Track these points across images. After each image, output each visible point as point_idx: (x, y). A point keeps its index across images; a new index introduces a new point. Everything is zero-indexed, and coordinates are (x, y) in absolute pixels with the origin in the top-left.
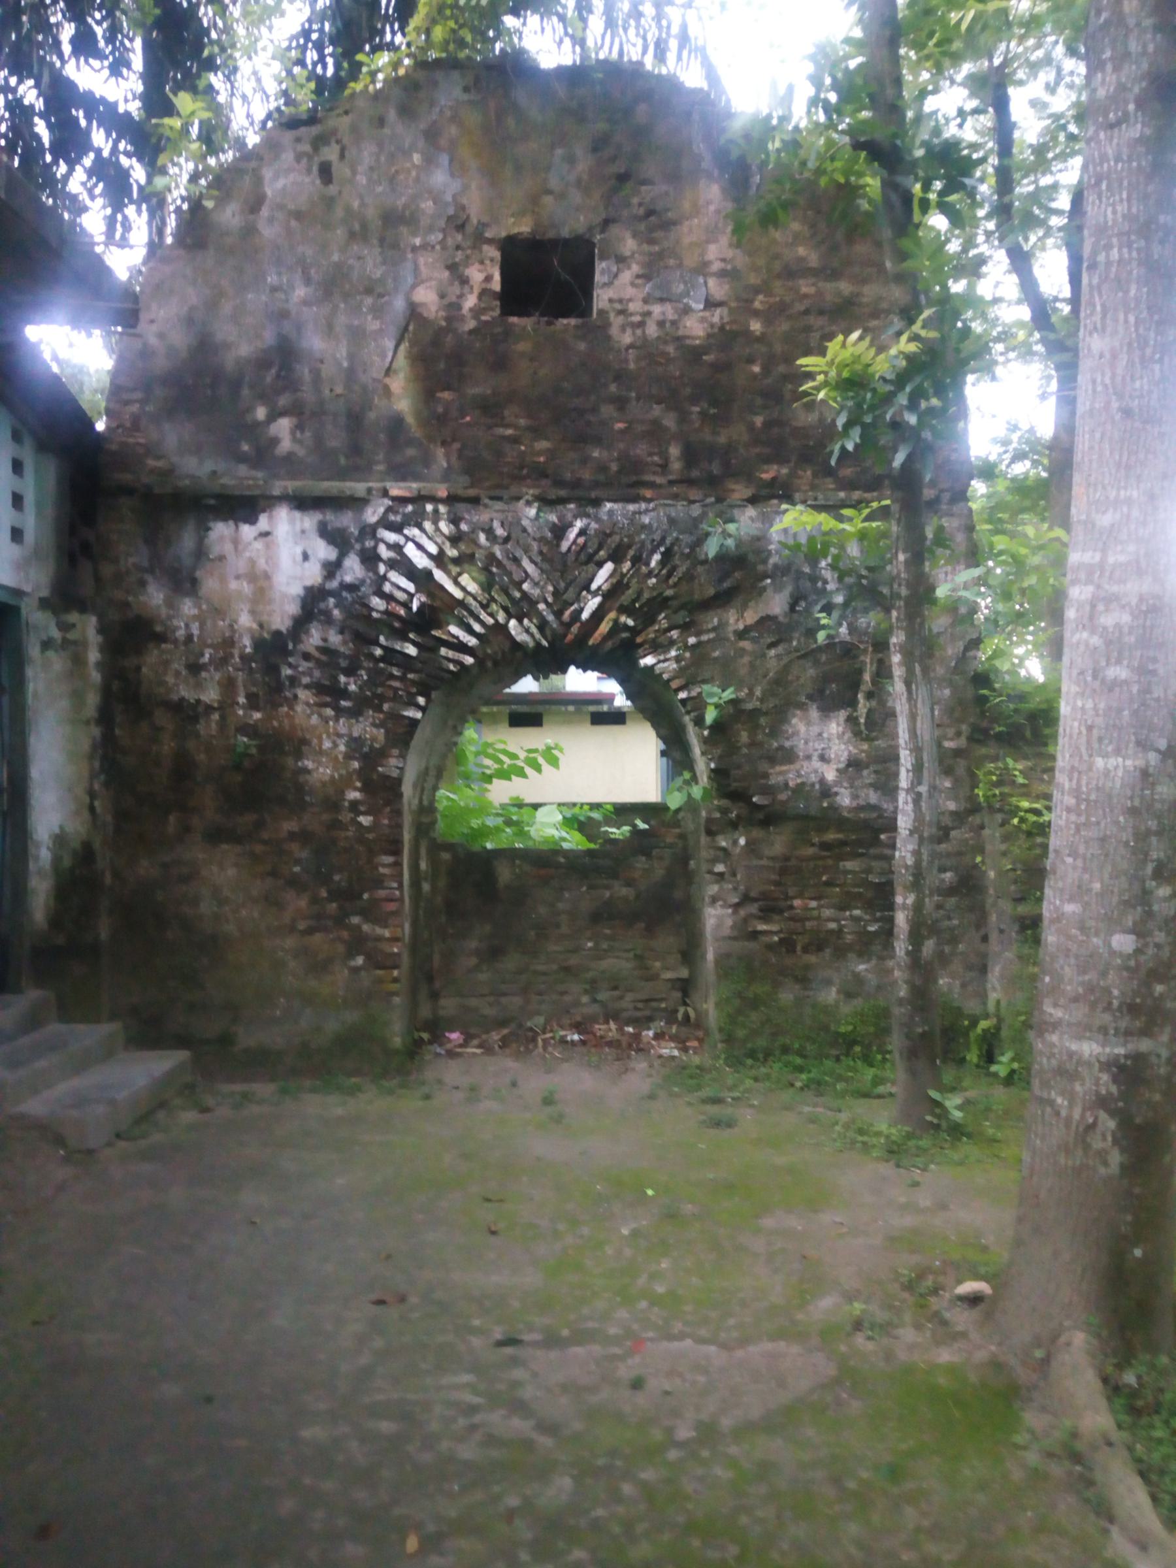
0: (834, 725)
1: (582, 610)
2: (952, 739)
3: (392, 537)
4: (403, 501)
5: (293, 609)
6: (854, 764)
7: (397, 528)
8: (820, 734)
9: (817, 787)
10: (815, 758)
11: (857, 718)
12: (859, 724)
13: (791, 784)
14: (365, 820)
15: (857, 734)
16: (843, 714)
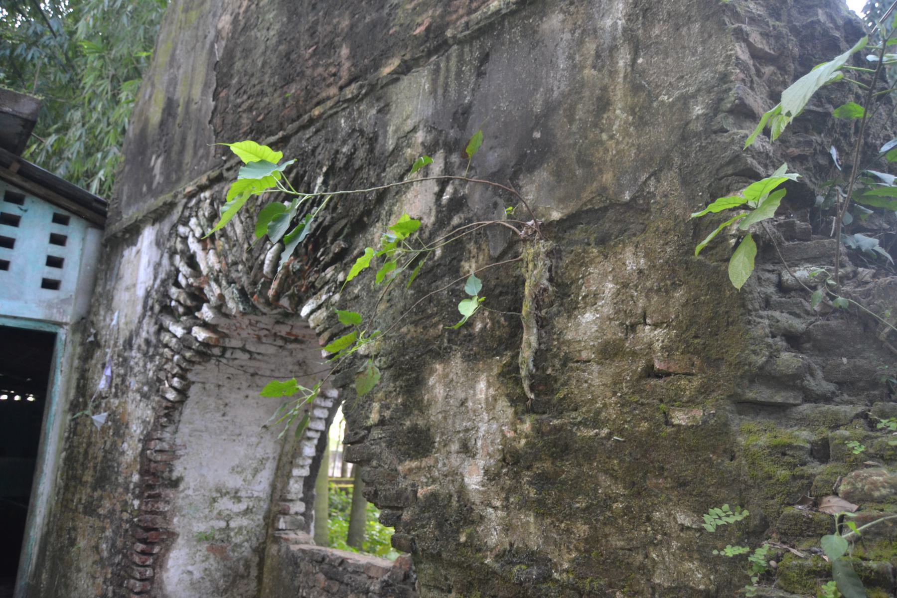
0: (482, 385)
1: (263, 262)
2: (692, 402)
3: (182, 230)
4: (191, 196)
5: (139, 309)
6: (512, 460)
7: (186, 223)
8: (463, 403)
9: (454, 503)
10: (455, 447)
11: (517, 369)
12: (518, 382)
13: (421, 492)
14: (136, 503)
15: (516, 400)
16: (498, 363)
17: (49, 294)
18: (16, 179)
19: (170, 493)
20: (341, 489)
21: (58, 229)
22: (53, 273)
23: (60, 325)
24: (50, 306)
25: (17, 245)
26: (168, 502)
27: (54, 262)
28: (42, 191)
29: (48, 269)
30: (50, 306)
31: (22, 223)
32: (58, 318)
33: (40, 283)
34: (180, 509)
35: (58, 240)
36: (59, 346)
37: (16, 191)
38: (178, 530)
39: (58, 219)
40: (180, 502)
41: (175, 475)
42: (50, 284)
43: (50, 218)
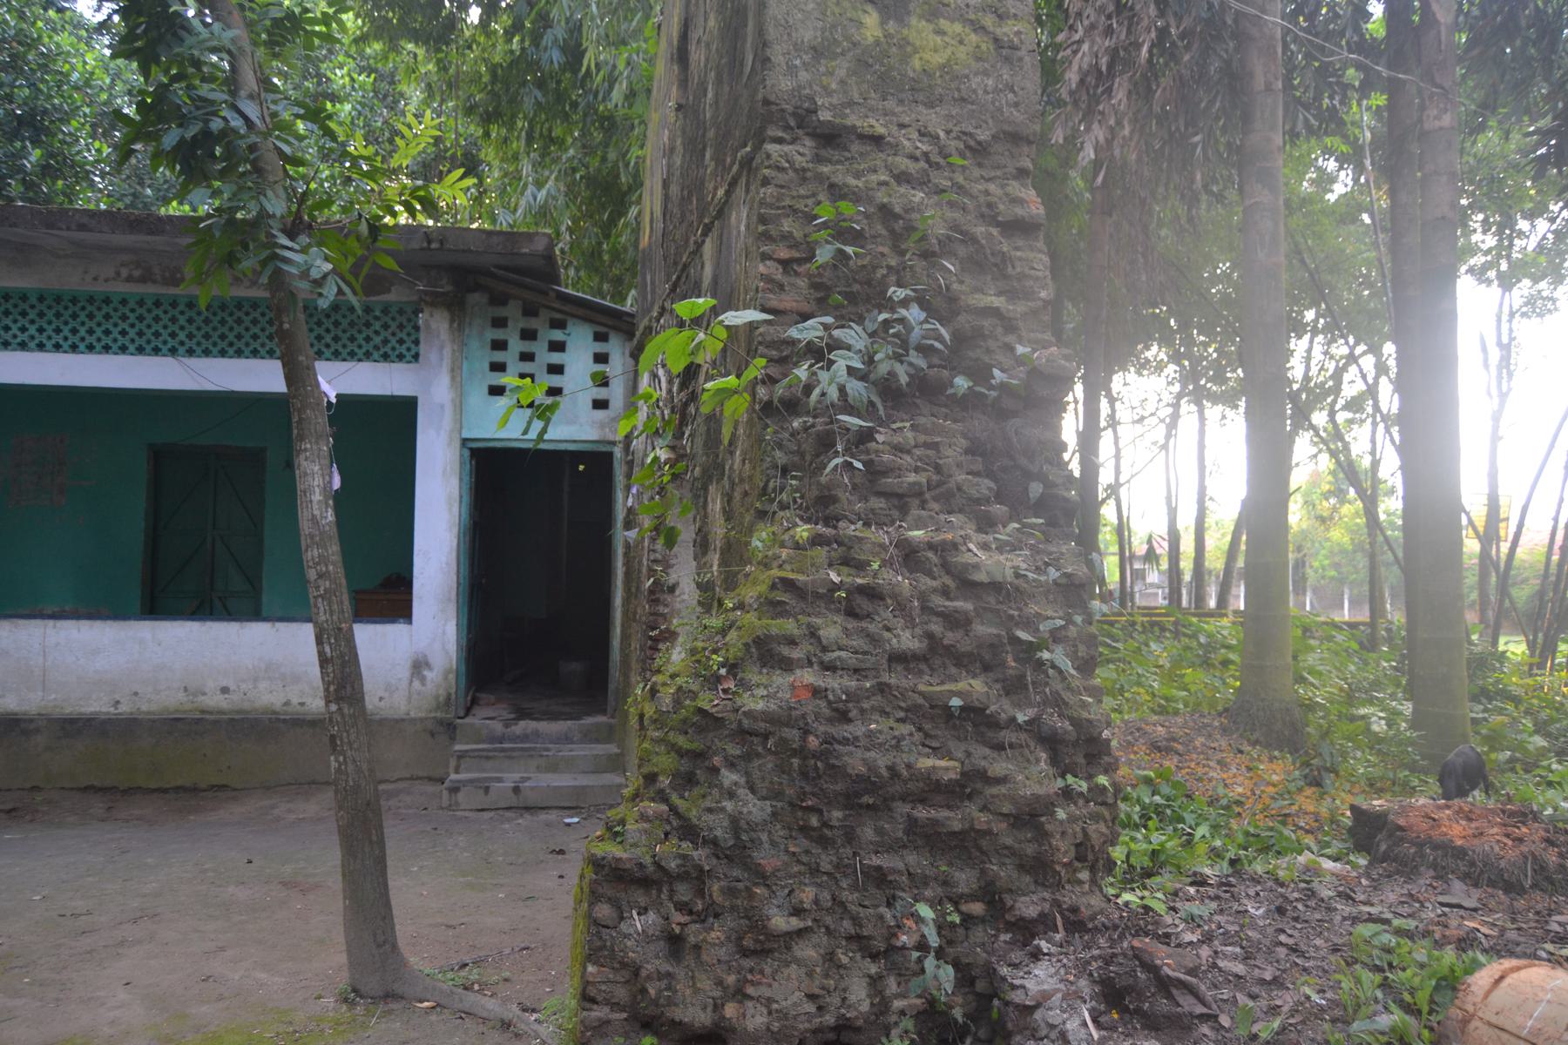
17: (600, 414)
18: (557, 305)
19: (669, 598)
20: (1153, 624)
21: (600, 347)
22: (601, 393)
23: (613, 443)
24: (602, 426)
25: (566, 369)
26: (666, 606)
27: (602, 381)
28: (581, 312)
29: (595, 390)
30: (602, 426)
31: (569, 347)
32: (611, 437)
33: (590, 405)
34: (679, 612)
35: (601, 358)
36: (616, 465)
37: (558, 316)
38: (678, 630)
39: (600, 337)
40: (678, 606)
41: (671, 581)
42: (600, 404)
43: (591, 337)
